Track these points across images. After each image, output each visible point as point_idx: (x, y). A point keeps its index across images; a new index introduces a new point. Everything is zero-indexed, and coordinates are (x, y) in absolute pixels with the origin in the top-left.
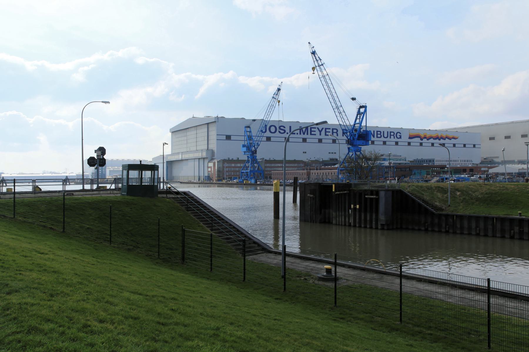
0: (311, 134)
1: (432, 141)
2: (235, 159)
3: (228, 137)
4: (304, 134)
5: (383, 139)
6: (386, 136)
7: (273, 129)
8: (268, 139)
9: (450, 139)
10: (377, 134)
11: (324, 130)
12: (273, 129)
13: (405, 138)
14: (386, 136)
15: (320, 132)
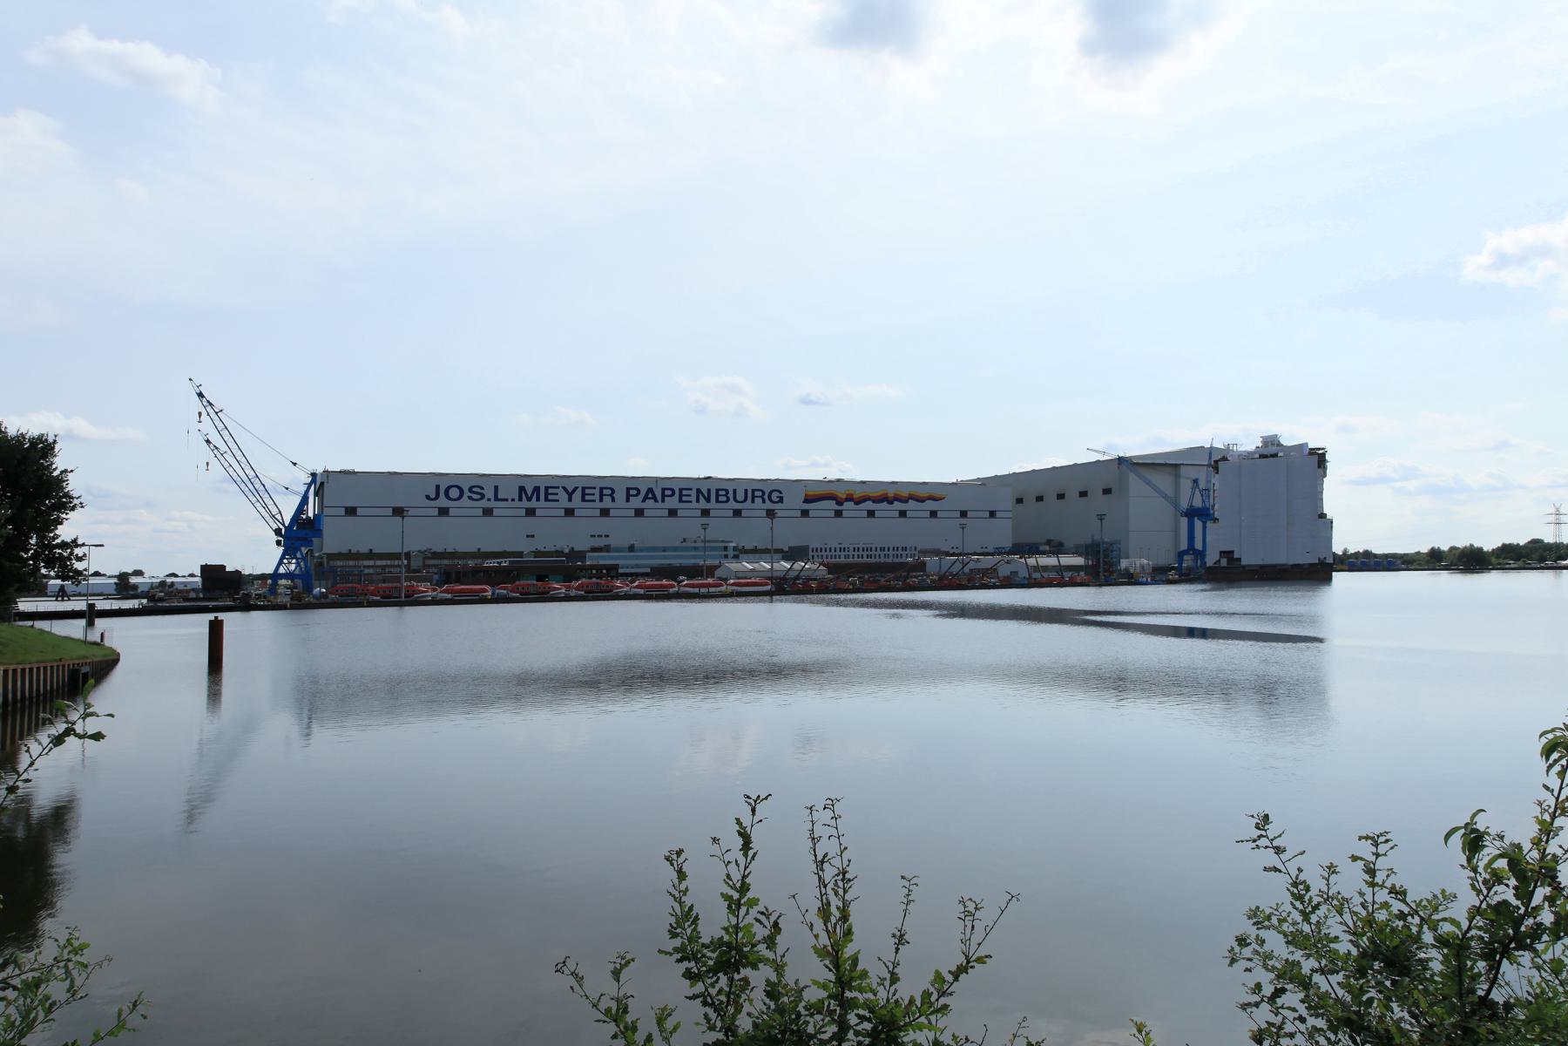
0: (546, 500)
1: (869, 505)
2: (364, 550)
3: (351, 511)
4: (529, 499)
5: (733, 505)
6: (740, 497)
7: (454, 493)
8: (444, 512)
9: (921, 500)
10: (717, 495)
11: (579, 492)
12: (454, 493)
13: (794, 502)
14: (740, 497)
15: (570, 495)
